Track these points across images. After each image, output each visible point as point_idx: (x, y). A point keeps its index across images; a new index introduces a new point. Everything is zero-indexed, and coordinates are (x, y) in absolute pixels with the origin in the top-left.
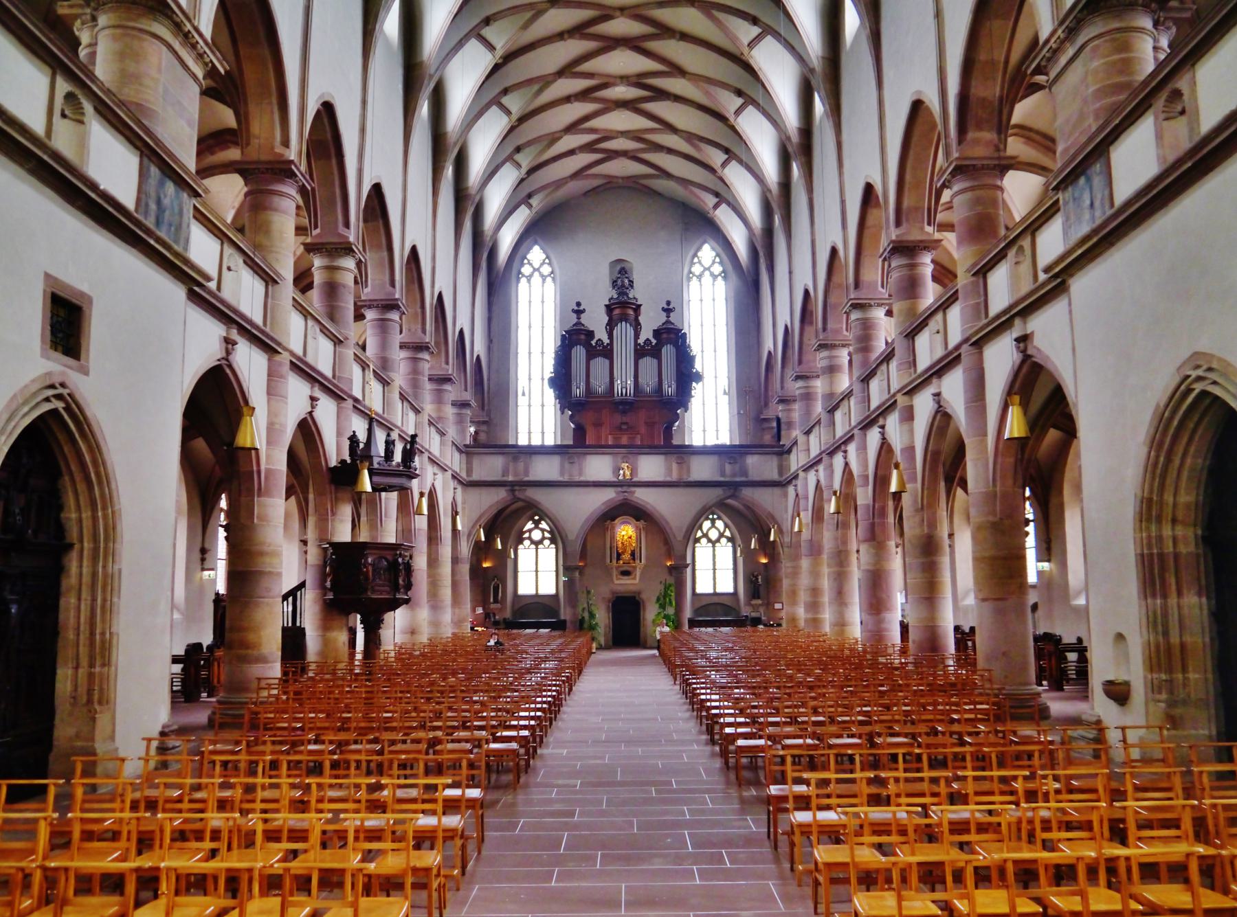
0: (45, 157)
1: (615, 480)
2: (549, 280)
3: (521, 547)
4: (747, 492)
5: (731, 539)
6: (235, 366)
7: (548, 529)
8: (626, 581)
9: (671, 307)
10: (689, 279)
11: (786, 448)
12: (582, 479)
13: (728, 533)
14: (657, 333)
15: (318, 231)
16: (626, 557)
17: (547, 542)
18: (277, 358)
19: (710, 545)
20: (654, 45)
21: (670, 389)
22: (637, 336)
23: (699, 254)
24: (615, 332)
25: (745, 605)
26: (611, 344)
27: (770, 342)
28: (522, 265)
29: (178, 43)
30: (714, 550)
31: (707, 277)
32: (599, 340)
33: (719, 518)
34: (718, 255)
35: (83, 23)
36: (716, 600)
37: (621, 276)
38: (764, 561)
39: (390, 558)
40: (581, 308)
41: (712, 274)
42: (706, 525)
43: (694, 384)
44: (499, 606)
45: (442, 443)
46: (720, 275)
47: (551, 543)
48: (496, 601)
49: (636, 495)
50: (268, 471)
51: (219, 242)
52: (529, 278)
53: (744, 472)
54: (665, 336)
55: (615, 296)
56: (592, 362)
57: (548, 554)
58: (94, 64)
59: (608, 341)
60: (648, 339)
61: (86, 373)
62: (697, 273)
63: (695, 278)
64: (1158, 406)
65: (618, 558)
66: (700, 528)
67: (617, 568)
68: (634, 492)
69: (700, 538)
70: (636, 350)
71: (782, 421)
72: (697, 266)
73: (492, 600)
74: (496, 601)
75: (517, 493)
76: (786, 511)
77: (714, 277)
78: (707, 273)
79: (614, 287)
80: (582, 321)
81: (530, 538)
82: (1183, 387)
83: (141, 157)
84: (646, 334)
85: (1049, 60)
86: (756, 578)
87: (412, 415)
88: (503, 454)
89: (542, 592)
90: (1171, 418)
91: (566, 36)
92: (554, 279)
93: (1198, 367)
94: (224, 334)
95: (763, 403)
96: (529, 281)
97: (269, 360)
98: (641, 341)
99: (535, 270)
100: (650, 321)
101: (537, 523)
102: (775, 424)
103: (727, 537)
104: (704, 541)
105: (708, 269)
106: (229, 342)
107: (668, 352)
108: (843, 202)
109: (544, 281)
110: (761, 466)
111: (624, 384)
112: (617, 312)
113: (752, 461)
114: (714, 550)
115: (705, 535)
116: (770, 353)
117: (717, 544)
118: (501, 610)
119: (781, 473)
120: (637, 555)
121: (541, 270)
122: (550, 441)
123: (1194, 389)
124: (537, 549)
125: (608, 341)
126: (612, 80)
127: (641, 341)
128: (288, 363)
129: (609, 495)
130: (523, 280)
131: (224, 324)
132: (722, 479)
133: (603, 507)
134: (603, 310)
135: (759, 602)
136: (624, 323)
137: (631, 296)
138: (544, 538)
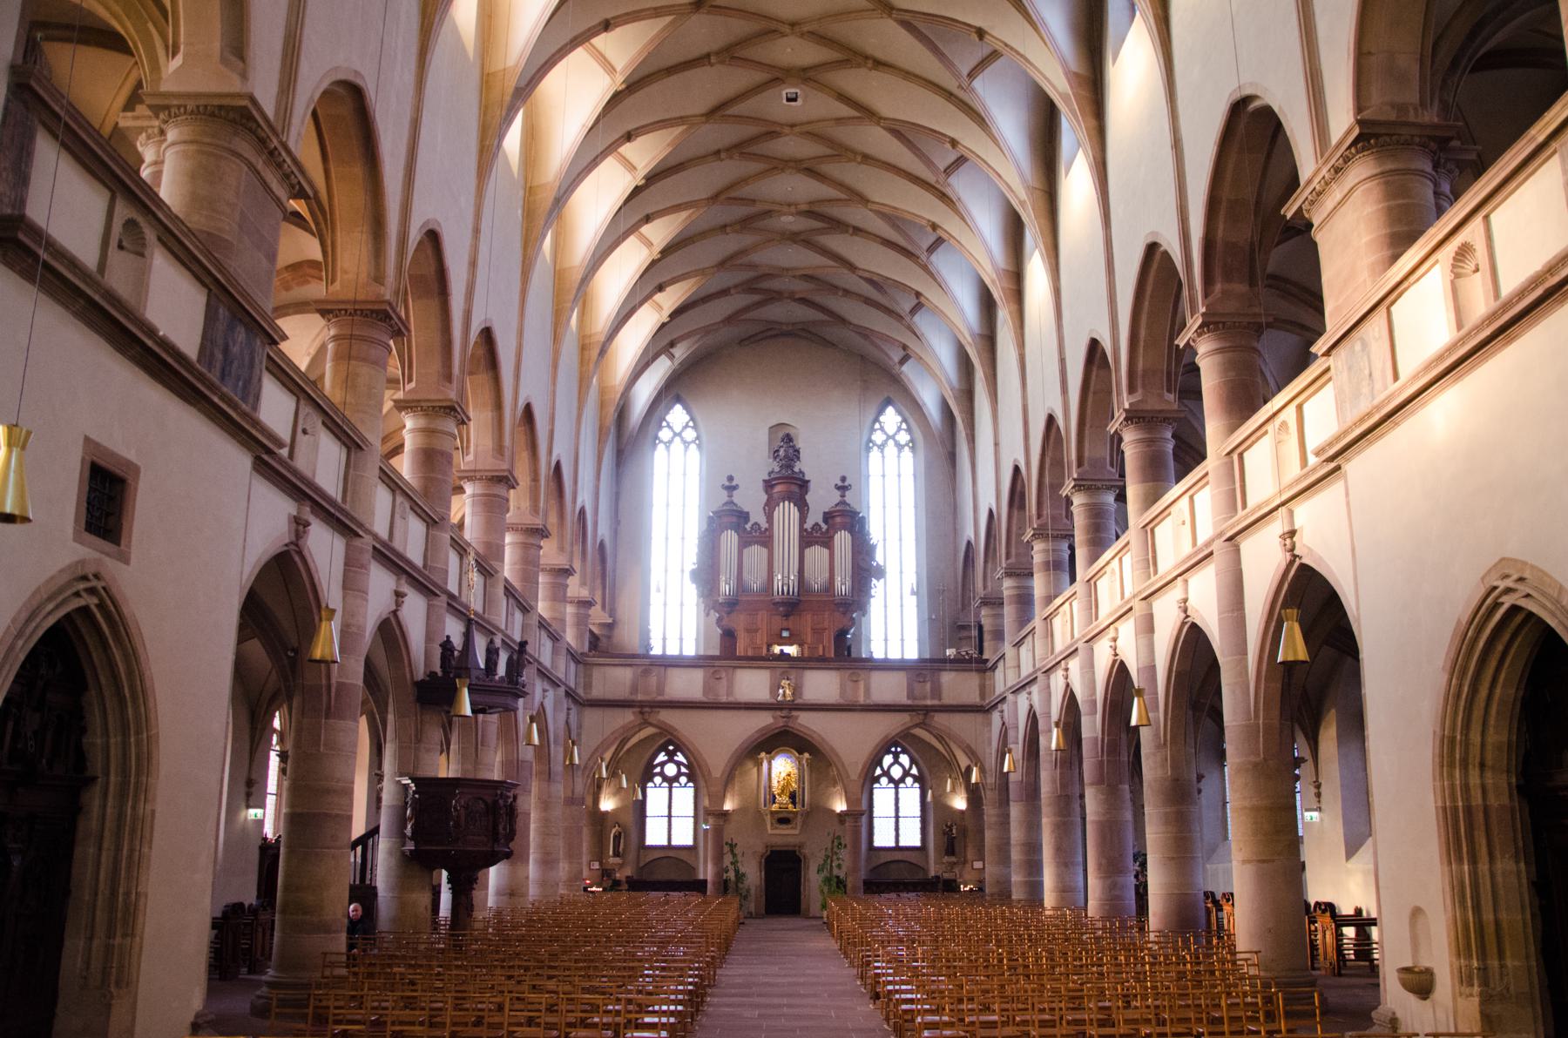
0: (97, 298)
1: (773, 701)
2: (693, 447)
4: (940, 719)
6: (306, 553)
7: (685, 761)
8: (784, 830)
9: (846, 484)
10: (868, 449)
11: (990, 665)
12: (731, 699)
13: (914, 771)
14: (828, 517)
15: (413, 384)
17: (683, 780)
18: (357, 542)
19: (892, 785)
20: (833, 169)
21: (842, 585)
22: (803, 520)
23: (882, 418)
24: (776, 513)
26: (770, 528)
27: (972, 529)
28: (660, 427)
29: (261, 162)
30: (897, 794)
31: (891, 448)
32: (756, 523)
33: (904, 752)
34: (905, 420)
35: (149, 138)
36: (898, 856)
37: (786, 448)
38: (960, 803)
39: (489, 800)
40: (734, 483)
42: (888, 759)
43: (874, 581)
44: (618, 860)
45: (555, 651)
46: (907, 445)
50: (340, 685)
51: (295, 398)
52: (668, 444)
53: (937, 691)
54: (838, 520)
55: (777, 469)
57: (684, 796)
58: (159, 185)
59: (766, 526)
60: (817, 524)
61: (127, 562)
62: (879, 442)
63: (875, 448)
64: (1459, 622)
66: (880, 763)
68: (797, 718)
69: (880, 776)
70: (801, 537)
72: (879, 432)
73: (611, 853)
74: (616, 854)
75: (646, 716)
76: (990, 744)
77: (900, 447)
78: (891, 442)
79: (775, 458)
80: (735, 500)
81: (662, 774)
82: (1489, 601)
83: (209, 296)
84: (815, 517)
85: (1312, 203)
86: (950, 828)
87: (518, 616)
88: (630, 665)
90: (1475, 639)
91: (723, 155)
92: (699, 447)
93: (1507, 576)
94: (295, 513)
95: (960, 606)
96: (668, 448)
97: (348, 546)
98: (808, 526)
99: (676, 434)
100: (821, 499)
101: (671, 755)
102: (974, 633)
103: (913, 776)
104: (884, 780)
105: (893, 437)
106: (299, 525)
107: (842, 539)
108: (1062, 361)
109: (686, 448)
110: (958, 686)
111: (784, 581)
112: (778, 489)
113: (947, 678)
114: (897, 794)
115: (886, 773)
116: (969, 543)
117: (902, 785)
118: (621, 866)
119: (983, 695)
121: (684, 434)
122: (690, 650)
123: (1503, 603)
124: (670, 788)
125: (766, 526)
126: (777, 208)
127: (808, 526)
128: (371, 549)
129: (765, 720)
130: (661, 447)
131: (296, 500)
132: (909, 702)
133: (757, 736)
134: (761, 485)
135: (953, 859)
137: (796, 470)
138: (679, 774)
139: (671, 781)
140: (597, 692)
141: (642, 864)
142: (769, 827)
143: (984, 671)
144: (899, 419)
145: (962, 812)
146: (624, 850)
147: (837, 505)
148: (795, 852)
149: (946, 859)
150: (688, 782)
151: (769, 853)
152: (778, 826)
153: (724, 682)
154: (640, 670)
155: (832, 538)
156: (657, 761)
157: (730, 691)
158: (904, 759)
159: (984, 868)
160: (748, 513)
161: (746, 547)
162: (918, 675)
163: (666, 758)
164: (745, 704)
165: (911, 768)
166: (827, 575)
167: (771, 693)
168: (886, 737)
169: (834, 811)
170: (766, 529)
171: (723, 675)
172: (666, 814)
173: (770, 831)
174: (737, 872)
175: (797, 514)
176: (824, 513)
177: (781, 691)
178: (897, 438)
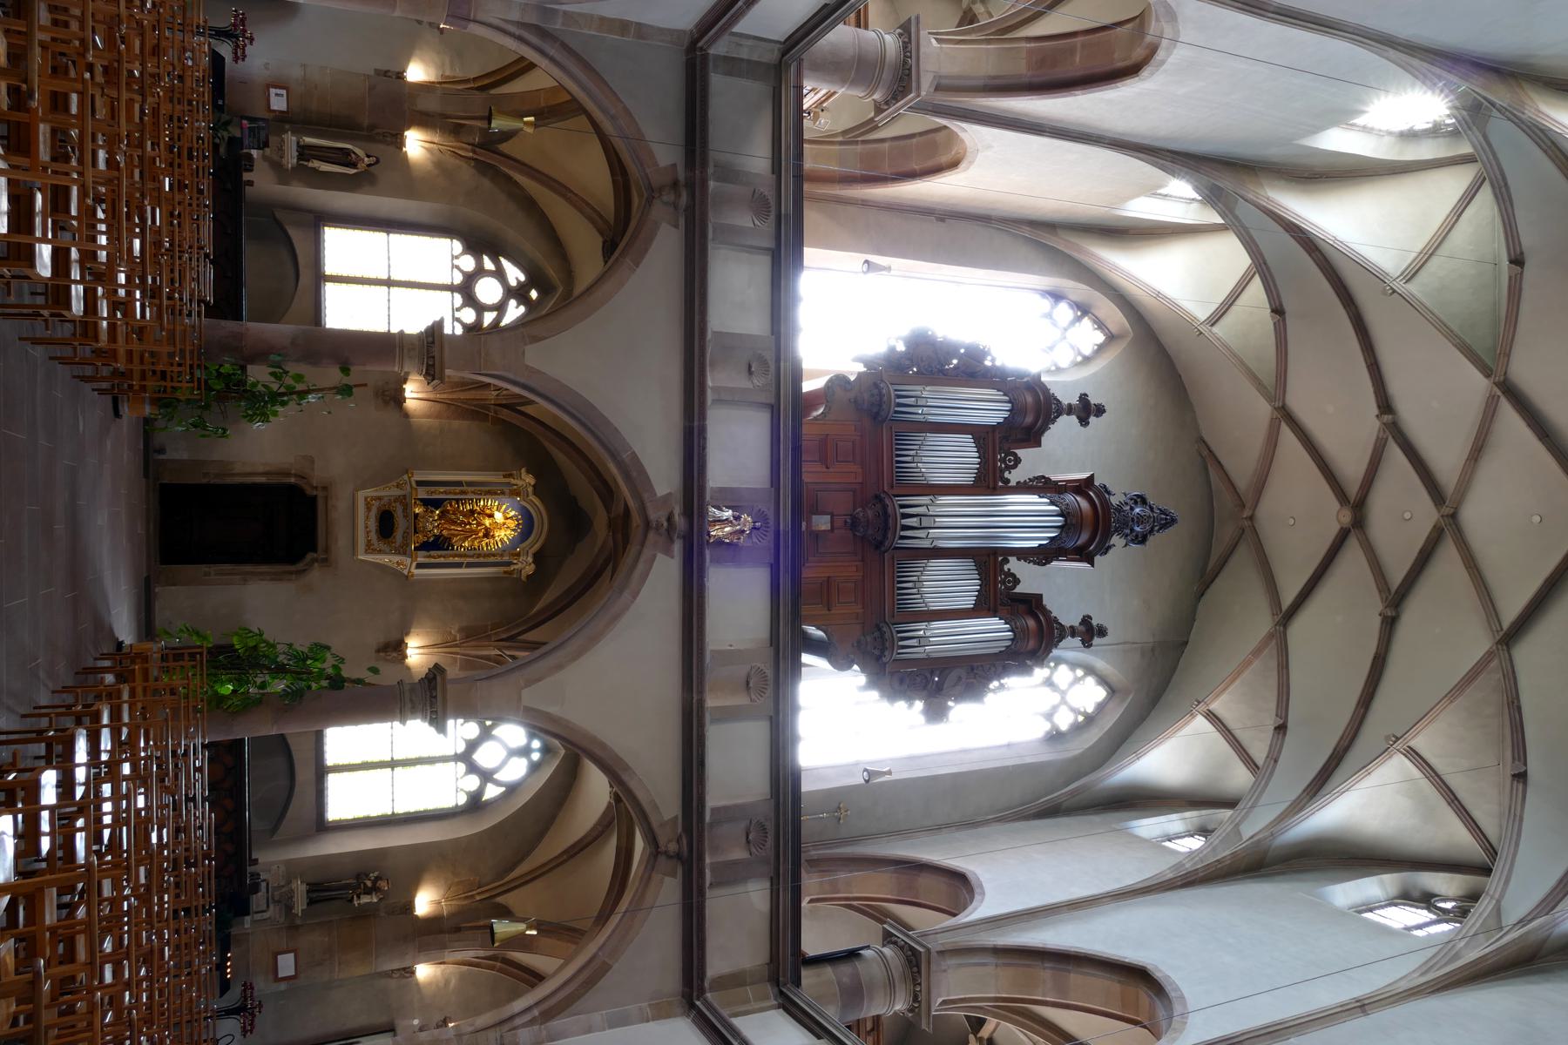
1: (708, 498)
3: (457, 246)
5: (475, 804)
8: (365, 523)
13: (492, 792)
14: (1033, 604)
16: (433, 524)
17: (469, 316)
22: (1023, 554)
23: (1090, 680)
24: (1034, 498)
25: (288, 863)
30: (444, 759)
33: (534, 768)
36: (304, 774)
38: (425, 902)
43: (919, 705)
44: (291, 159)
47: (469, 329)
48: (305, 152)
49: (661, 558)
54: (1031, 623)
56: (968, 438)
59: (1013, 483)
65: (426, 503)
67: (403, 500)
68: (668, 552)
70: (995, 551)
71: (859, 965)
73: (309, 140)
74: (305, 152)
75: (668, 197)
81: (480, 272)
84: (1029, 578)
86: (374, 889)
89: (332, 294)
98: (1014, 565)
101: (519, 293)
105: (1064, 701)
107: (992, 629)
114: (444, 759)
118: (277, 166)
120: (437, 556)
125: (1013, 483)
127: (1014, 565)
135: (300, 905)
138: (480, 308)
139: (466, 289)
140: (723, 89)
141: (279, 215)
142: (370, 492)
143: (775, 980)
144: (1090, 709)
145: (409, 907)
146: (315, 170)
147: (1056, 620)
148: (315, 550)
149: (300, 888)
150: (464, 326)
151: (309, 491)
152: (374, 512)
153: (742, 382)
154: (768, 191)
155: (993, 613)
156: (505, 263)
157: (732, 399)
158: (516, 770)
159: (277, 980)
160: (1039, 444)
162: (763, 828)
163: (513, 283)
164: (702, 430)
165: (498, 783)
166: (935, 606)
167: (722, 490)
168: (627, 768)
169: (407, 634)
170: (1008, 481)
171: (758, 381)
172: (395, 277)
173: (361, 495)
174: (275, 398)
175: (1035, 544)
176: (1039, 597)
178: (1063, 709)
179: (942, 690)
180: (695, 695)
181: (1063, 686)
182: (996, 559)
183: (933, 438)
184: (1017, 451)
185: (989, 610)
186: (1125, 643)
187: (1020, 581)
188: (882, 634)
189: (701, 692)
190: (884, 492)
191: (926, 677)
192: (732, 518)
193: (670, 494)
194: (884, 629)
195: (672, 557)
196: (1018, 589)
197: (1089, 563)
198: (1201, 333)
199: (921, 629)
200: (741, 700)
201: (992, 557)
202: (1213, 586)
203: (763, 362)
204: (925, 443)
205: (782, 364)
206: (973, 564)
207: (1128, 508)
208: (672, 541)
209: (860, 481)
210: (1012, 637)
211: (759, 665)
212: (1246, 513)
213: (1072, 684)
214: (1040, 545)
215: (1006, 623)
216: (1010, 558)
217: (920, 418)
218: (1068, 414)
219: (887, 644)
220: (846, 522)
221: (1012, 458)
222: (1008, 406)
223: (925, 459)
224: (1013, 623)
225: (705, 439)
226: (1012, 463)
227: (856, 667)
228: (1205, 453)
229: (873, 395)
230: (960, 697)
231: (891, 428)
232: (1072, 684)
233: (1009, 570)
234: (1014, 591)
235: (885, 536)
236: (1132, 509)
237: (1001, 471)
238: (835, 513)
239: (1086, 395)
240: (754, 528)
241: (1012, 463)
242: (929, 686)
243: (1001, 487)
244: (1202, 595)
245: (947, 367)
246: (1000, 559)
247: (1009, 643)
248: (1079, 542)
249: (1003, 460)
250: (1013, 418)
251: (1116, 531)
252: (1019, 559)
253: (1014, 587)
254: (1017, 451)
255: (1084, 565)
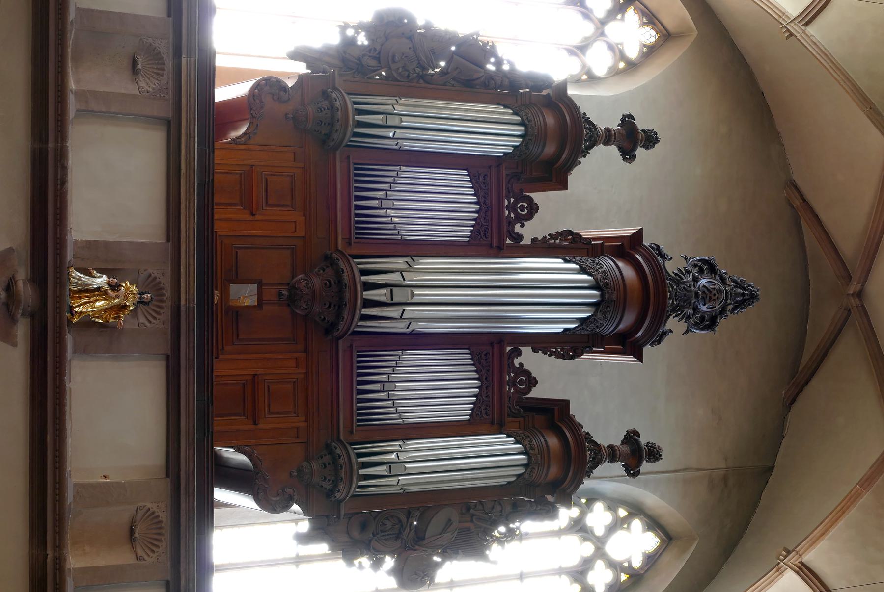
1: (69, 256)
22: (541, 343)
23: (637, 524)
24: (558, 263)
41: (587, 564)
54: (553, 442)
56: (461, 175)
59: (526, 241)
60: (532, 382)
70: (501, 339)
78: (589, 549)
98: (528, 358)
105: (600, 553)
125: (526, 241)
127: (528, 358)
136: (593, 295)
144: (637, 563)
160: (564, 186)
161: (474, 179)
164: (61, 156)
166: (412, 418)
167: (90, 245)
170: (520, 237)
171: (147, 84)
175: (558, 328)
176: (564, 405)
177: (101, 280)
178: (600, 564)
179: (423, 539)
180: (50, 552)
181: (599, 531)
182: (502, 349)
183: (410, 174)
184: (532, 195)
185: (492, 423)
186: (685, 470)
187: (537, 382)
188: (335, 459)
189: (59, 546)
190: (337, 250)
191: (400, 521)
192: (106, 287)
193: (10, 250)
194: (338, 451)
195: (14, 345)
196: (535, 393)
197: (635, 357)
198: (791, 35)
199: (393, 452)
200: (122, 557)
201: (496, 347)
202: (808, 389)
203: (156, 57)
204: (399, 180)
205: (184, 61)
206: (469, 356)
207: (690, 278)
208: (12, 319)
209: (303, 234)
210: (526, 462)
211: (149, 505)
212: (853, 288)
213: (611, 529)
214: (566, 330)
215: (517, 442)
216: (522, 348)
217: (391, 144)
218: (606, 143)
219: (343, 474)
220: (280, 294)
221: (526, 205)
222: (519, 130)
223: (397, 204)
224: (527, 443)
225: (64, 168)
226: (526, 211)
227: (295, 507)
228: (797, 202)
229: (320, 110)
230: (453, 549)
231: (348, 157)
232: (611, 529)
233: (521, 365)
234: (531, 395)
235: (339, 316)
236: (696, 280)
237: (510, 222)
238: (264, 281)
239: (631, 117)
240: (141, 302)
241: (526, 211)
242: (405, 534)
243: (509, 246)
244: (793, 401)
245: (430, 71)
246: (508, 349)
247: (520, 471)
248: (621, 326)
249: (512, 208)
250: (527, 147)
251: (673, 310)
252: (535, 350)
253: (529, 390)
254: (532, 195)
255: (631, 359)
